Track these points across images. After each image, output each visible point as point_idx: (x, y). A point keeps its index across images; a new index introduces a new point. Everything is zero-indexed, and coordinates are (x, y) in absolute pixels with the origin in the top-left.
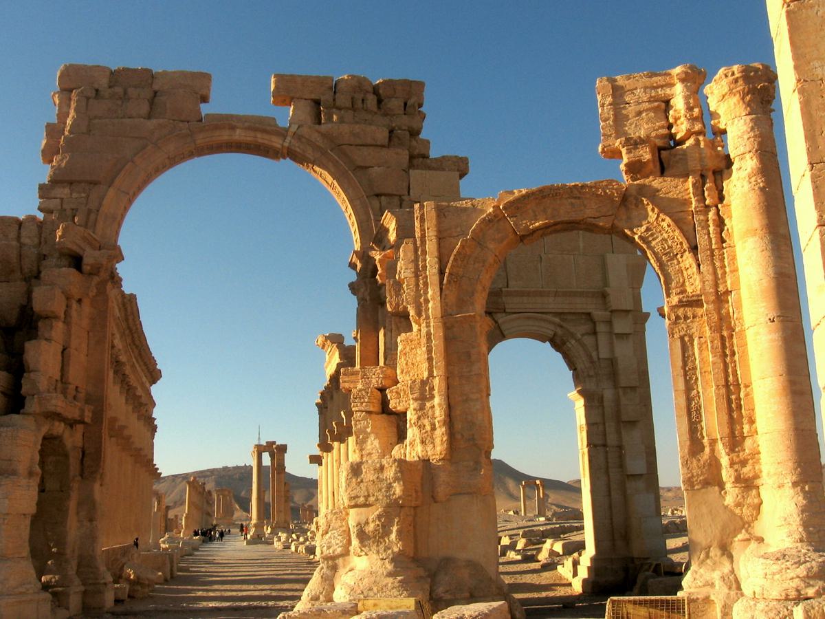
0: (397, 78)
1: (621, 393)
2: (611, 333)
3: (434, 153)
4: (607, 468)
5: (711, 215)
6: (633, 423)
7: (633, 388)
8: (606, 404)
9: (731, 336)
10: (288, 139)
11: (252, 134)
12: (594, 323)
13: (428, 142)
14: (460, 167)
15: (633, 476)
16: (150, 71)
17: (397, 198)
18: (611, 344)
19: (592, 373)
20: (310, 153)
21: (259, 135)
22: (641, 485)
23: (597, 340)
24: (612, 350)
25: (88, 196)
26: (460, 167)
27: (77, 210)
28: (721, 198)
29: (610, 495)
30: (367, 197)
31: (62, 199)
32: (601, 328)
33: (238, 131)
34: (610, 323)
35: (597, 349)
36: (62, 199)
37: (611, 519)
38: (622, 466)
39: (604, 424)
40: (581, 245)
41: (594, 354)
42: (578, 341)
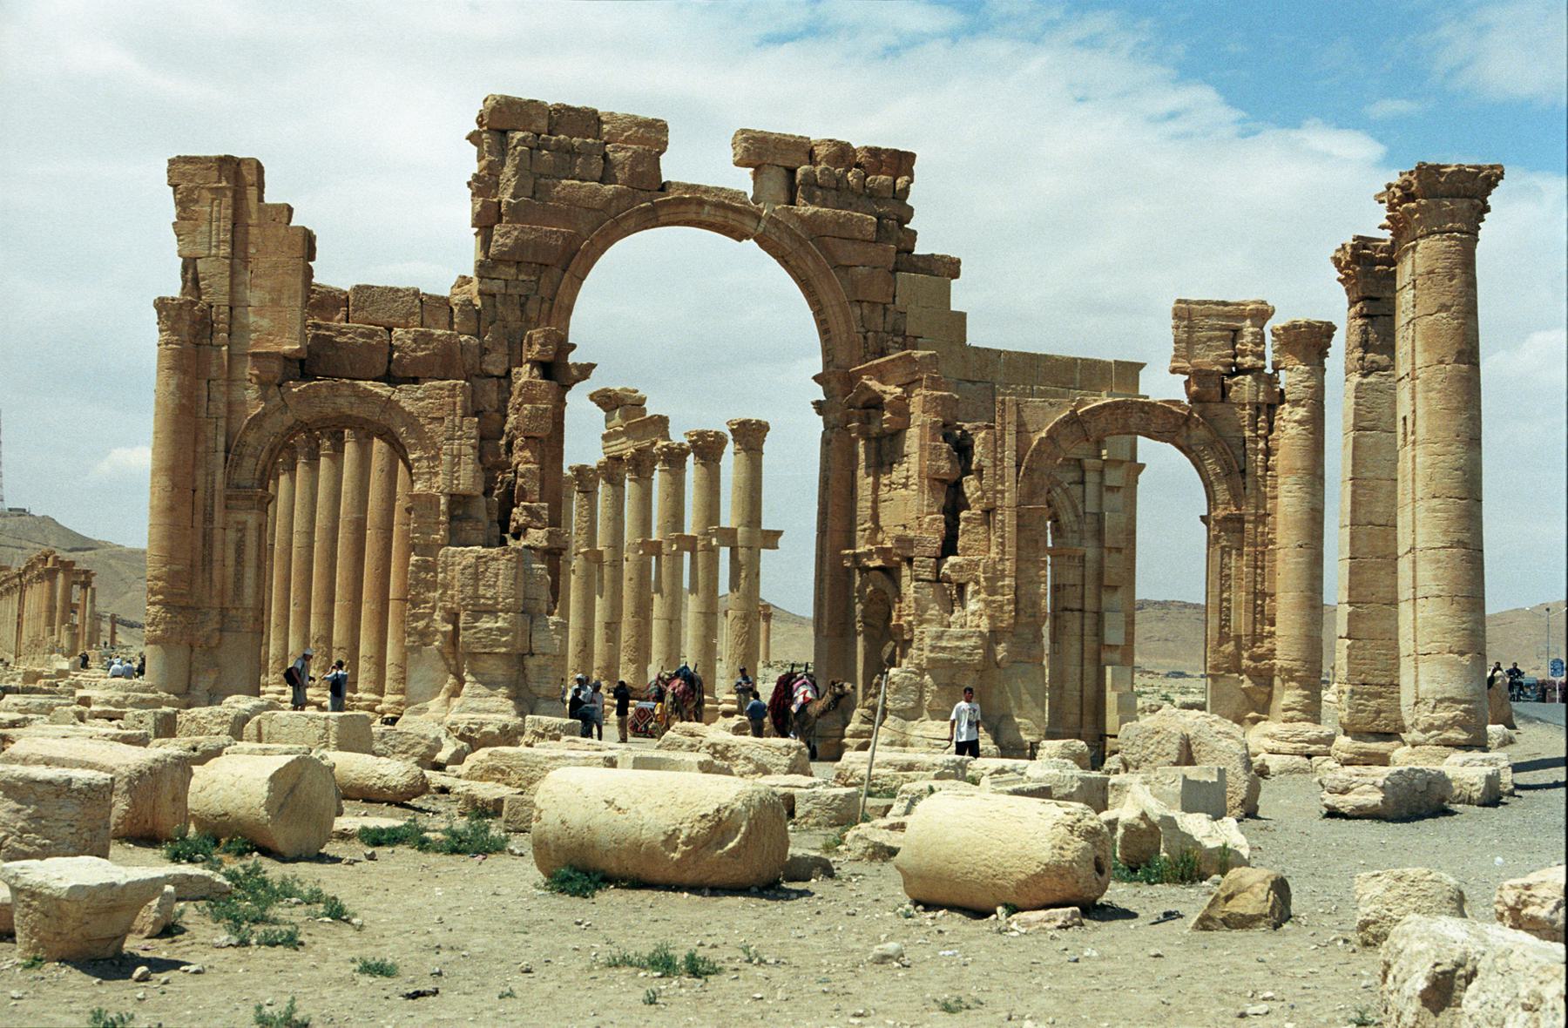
0: (884, 147)
1: (1106, 551)
2: (1101, 484)
3: (919, 249)
4: (1083, 635)
5: (1261, 445)
6: (1115, 588)
7: (1119, 550)
8: (1087, 565)
9: (1263, 553)
10: (763, 224)
11: (720, 212)
12: (1084, 472)
13: (915, 233)
14: (951, 268)
15: (1109, 646)
16: (595, 112)
17: (881, 307)
18: (1100, 497)
19: (1075, 528)
20: (787, 243)
21: (730, 215)
22: (1117, 656)
23: (1084, 491)
24: (1100, 505)
25: (539, 279)
26: (951, 268)
27: (527, 297)
28: (1271, 431)
29: (1082, 665)
30: (850, 302)
31: (506, 280)
32: (1091, 478)
33: (707, 208)
34: (1101, 473)
35: (1084, 501)
36: (506, 280)
37: (1082, 691)
38: (1099, 633)
39: (1083, 585)
40: (1078, 376)
41: (1080, 506)
42: (1065, 491)
